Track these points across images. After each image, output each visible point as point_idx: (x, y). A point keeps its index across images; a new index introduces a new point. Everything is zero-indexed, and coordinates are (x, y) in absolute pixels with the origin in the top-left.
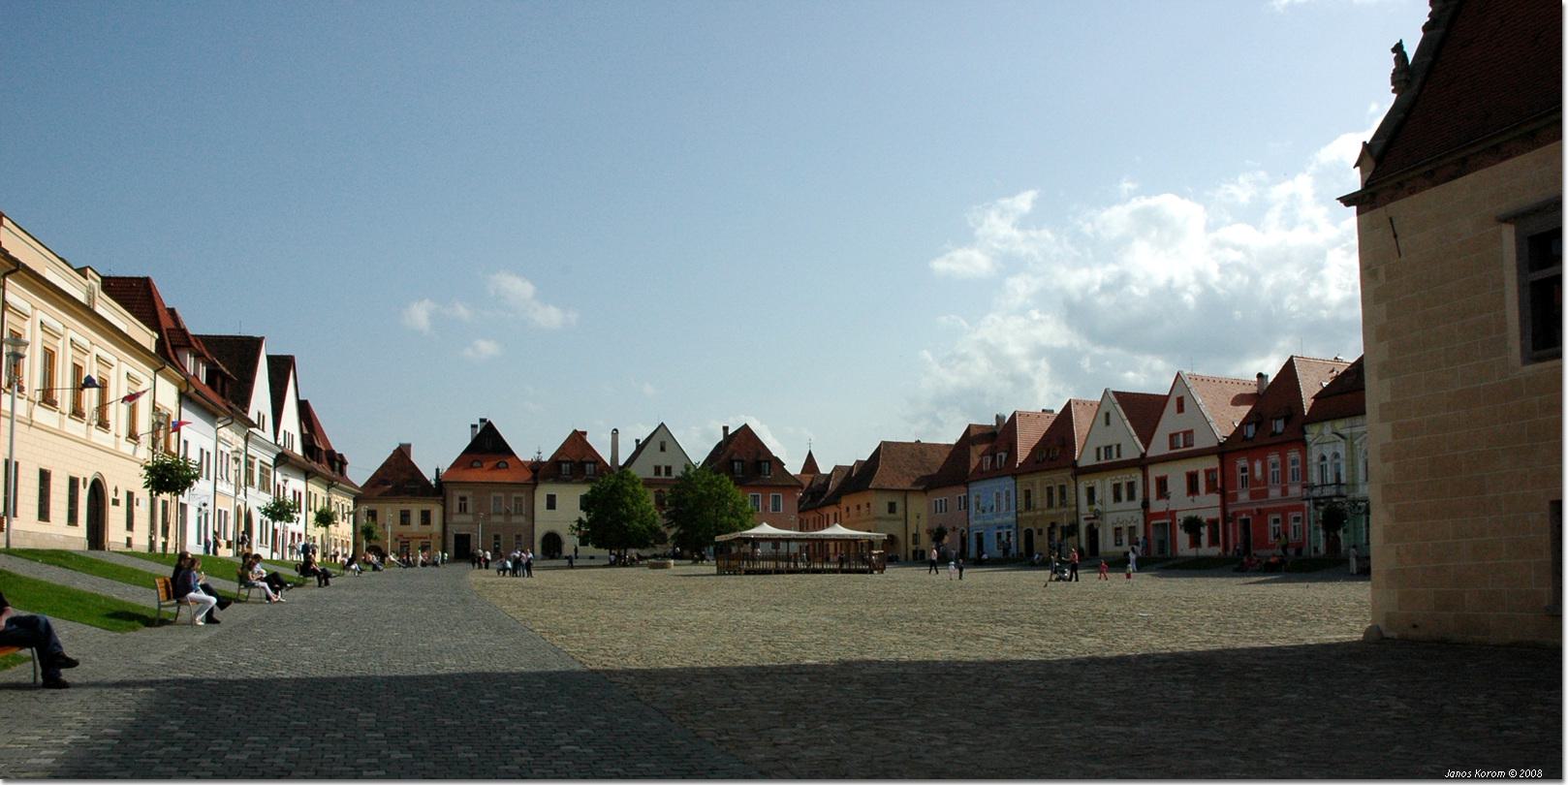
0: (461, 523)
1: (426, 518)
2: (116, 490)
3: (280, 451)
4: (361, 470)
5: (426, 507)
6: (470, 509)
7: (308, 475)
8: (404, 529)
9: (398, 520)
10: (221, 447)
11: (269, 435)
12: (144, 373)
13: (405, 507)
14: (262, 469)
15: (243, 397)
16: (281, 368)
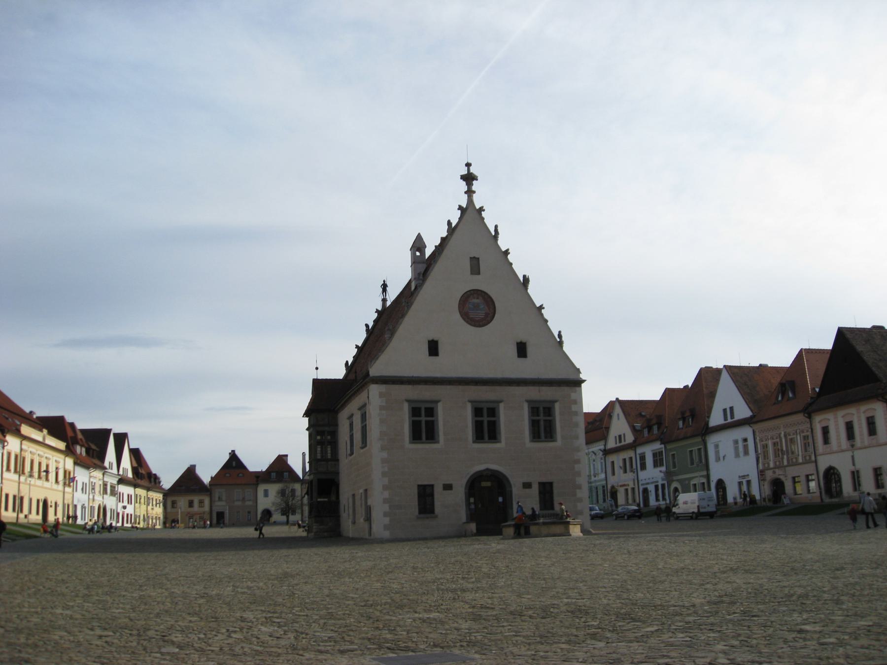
0: (220, 506)
1: (201, 502)
2: (51, 502)
3: (120, 477)
4: (167, 482)
5: (201, 498)
6: (224, 498)
7: (135, 486)
8: (191, 510)
9: (187, 504)
10: (92, 480)
11: (115, 471)
12: (60, 457)
13: (190, 498)
14: (111, 486)
15: (102, 456)
16: (121, 439)
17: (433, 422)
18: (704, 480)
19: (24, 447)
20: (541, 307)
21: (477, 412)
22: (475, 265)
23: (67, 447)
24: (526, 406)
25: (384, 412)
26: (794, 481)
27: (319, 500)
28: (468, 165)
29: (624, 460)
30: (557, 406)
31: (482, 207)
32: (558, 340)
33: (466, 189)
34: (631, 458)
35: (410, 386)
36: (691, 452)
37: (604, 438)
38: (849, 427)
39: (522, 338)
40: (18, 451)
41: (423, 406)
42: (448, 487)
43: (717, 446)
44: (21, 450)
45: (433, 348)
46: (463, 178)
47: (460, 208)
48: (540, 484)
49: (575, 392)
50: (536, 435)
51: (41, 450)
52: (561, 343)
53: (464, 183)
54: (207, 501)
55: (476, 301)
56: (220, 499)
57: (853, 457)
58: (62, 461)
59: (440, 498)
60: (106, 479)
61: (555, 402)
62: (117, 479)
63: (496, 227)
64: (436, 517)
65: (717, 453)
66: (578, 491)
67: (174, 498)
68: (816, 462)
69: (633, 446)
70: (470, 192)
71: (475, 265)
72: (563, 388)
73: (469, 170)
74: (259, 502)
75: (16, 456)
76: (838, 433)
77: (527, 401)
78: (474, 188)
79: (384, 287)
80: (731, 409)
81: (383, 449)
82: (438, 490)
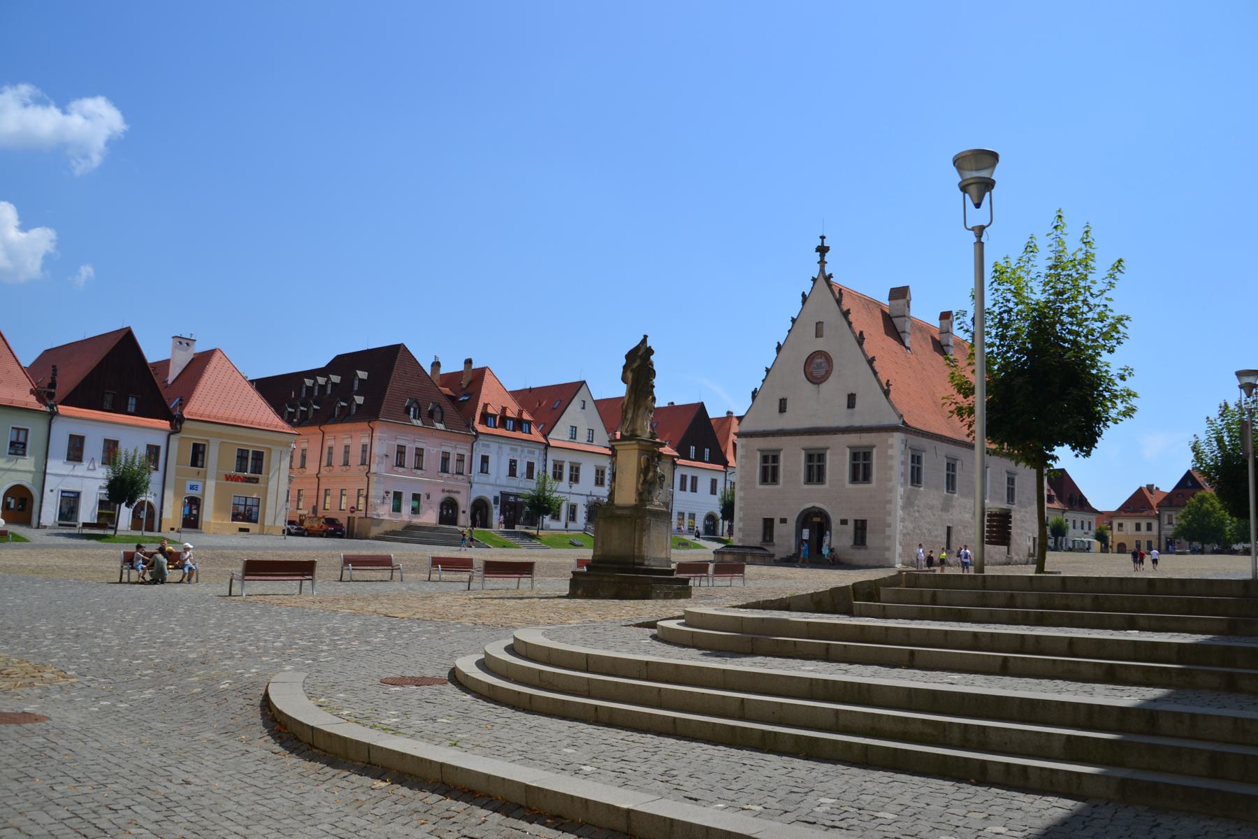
1: (1149, 527)
5: (1149, 521)
8: (1138, 533)
9: (1134, 528)
17: (777, 466)
20: (873, 359)
21: (810, 457)
22: (819, 330)
24: (848, 451)
25: (744, 460)
28: (823, 238)
30: (875, 451)
31: (831, 274)
32: (886, 388)
33: (819, 260)
35: (762, 438)
41: (771, 454)
42: (783, 521)
45: (783, 404)
48: (856, 521)
49: (892, 437)
50: (854, 479)
55: (819, 361)
56: (1170, 523)
59: (778, 528)
61: (874, 447)
64: (774, 545)
66: (887, 529)
67: (1120, 521)
70: (822, 262)
72: (881, 434)
73: (823, 243)
77: (849, 447)
78: (826, 260)
81: (741, 489)
82: (777, 522)
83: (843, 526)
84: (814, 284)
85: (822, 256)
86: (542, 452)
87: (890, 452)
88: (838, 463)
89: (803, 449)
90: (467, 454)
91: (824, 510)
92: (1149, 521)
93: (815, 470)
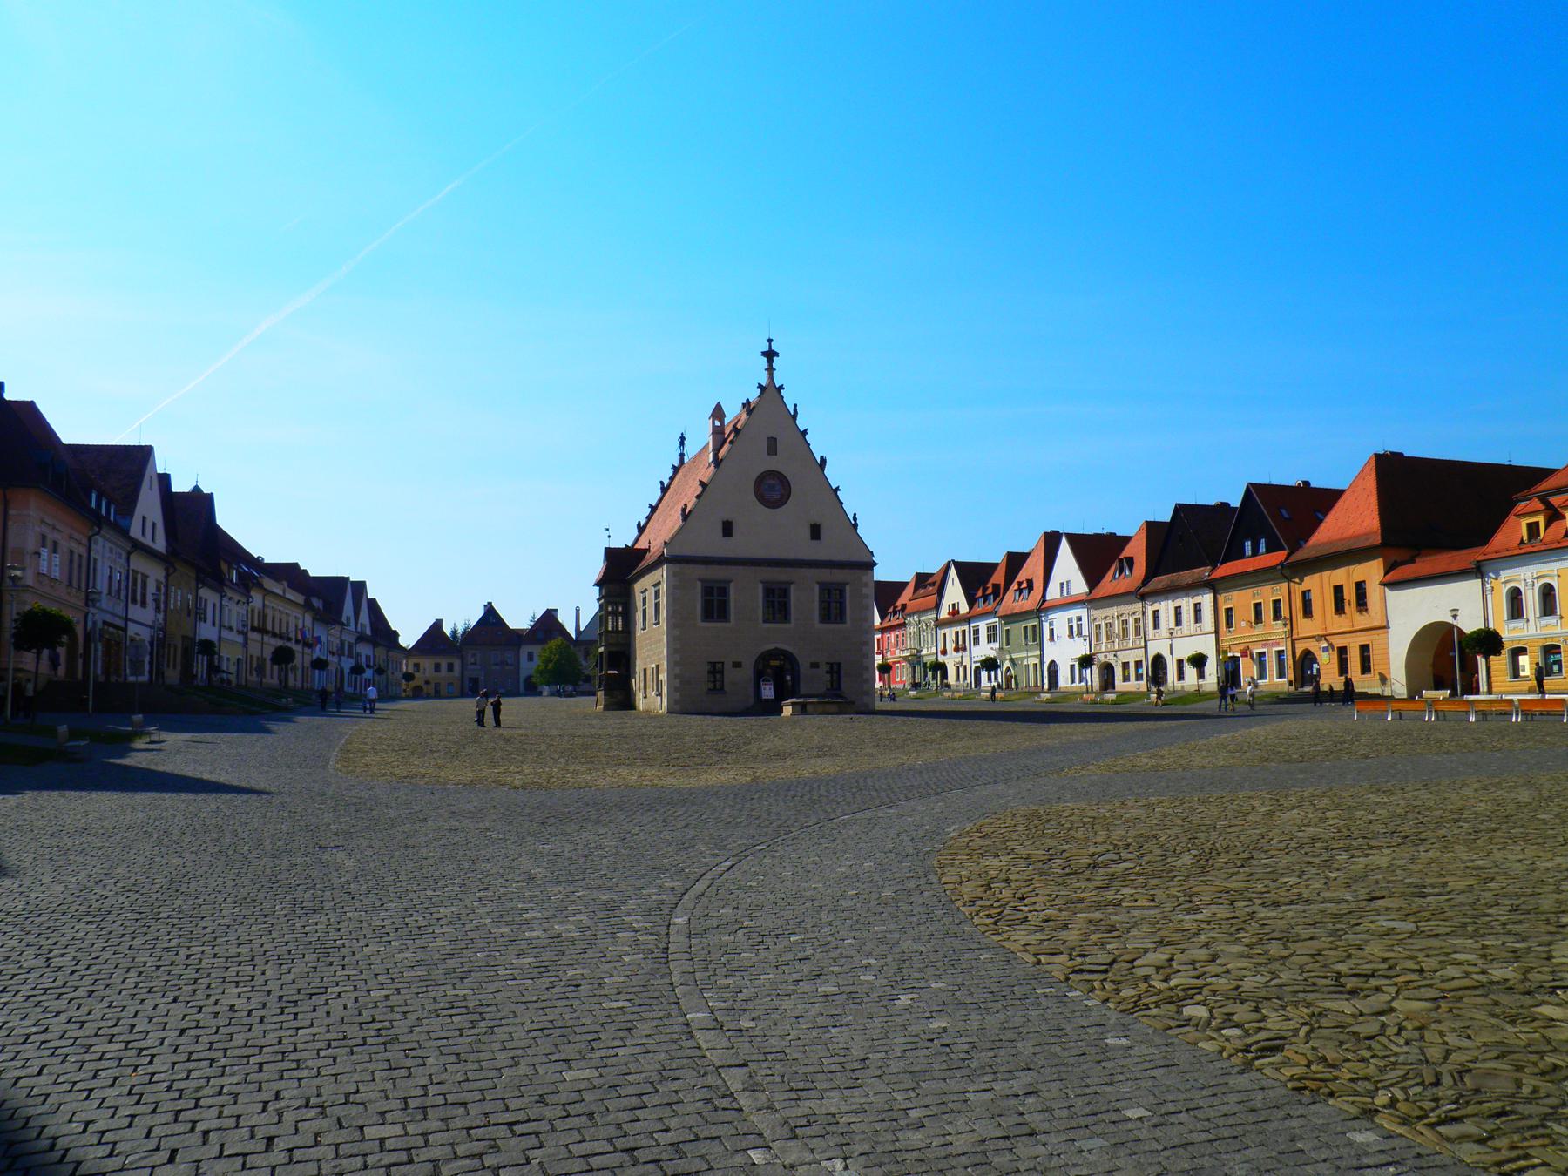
1: (450, 667)
5: (450, 661)
11: (352, 627)
12: (298, 613)
18: (1037, 661)
19: (266, 602)
20: (837, 489)
22: (772, 446)
23: (306, 601)
26: (1126, 665)
27: (609, 672)
28: (770, 341)
29: (957, 633)
30: (848, 588)
34: (964, 631)
35: (703, 567)
36: (1026, 628)
37: (938, 606)
38: (1178, 611)
39: (817, 520)
40: (261, 607)
42: (737, 665)
43: (1051, 624)
44: (264, 605)
45: (727, 529)
46: (764, 354)
47: (760, 386)
50: (826, 617)
51: (280, 606)
52: (855, 526)
53: (765, 359)
54: (457, 664)
57: (1171, 645)
58: (301, 617)
59: (731, 675)
60: (343, 638)
61: (847, 584)
62: (355, 637)
63: (795, 406)
65: (1052, 631)
68: (1146, 647)
69: (967, 619)
70: (770, 370)
71: (772, 446)
74: (521, 666)
75: (259, 612)
76: (1167, 618)
77: (818, 583)
79: (682, 440)
80: (1068, 582)
82: (728, 667)
83: (814, 670)
84: (762, 393)
85: (770, 361)
86: (124, 555)
87: (865, 591)
88: (805, 598)
89: (761, 582)
90: (85, 555)
91: (791, 654)
92: (450, 661)
93: (777, 603)
